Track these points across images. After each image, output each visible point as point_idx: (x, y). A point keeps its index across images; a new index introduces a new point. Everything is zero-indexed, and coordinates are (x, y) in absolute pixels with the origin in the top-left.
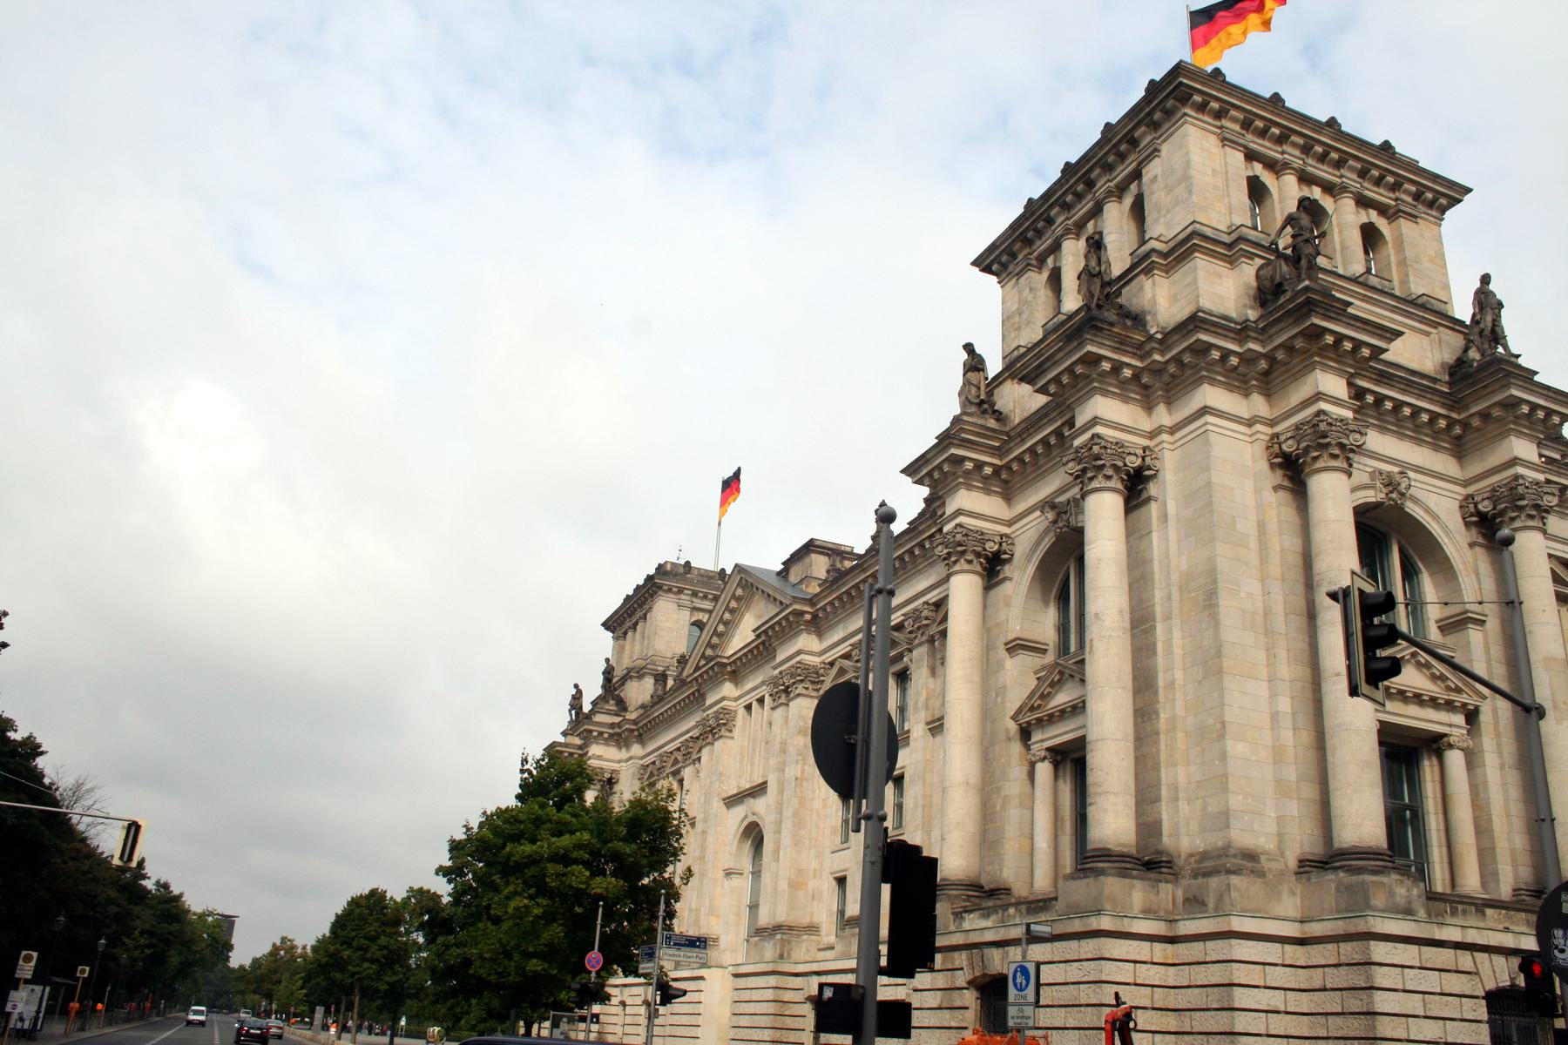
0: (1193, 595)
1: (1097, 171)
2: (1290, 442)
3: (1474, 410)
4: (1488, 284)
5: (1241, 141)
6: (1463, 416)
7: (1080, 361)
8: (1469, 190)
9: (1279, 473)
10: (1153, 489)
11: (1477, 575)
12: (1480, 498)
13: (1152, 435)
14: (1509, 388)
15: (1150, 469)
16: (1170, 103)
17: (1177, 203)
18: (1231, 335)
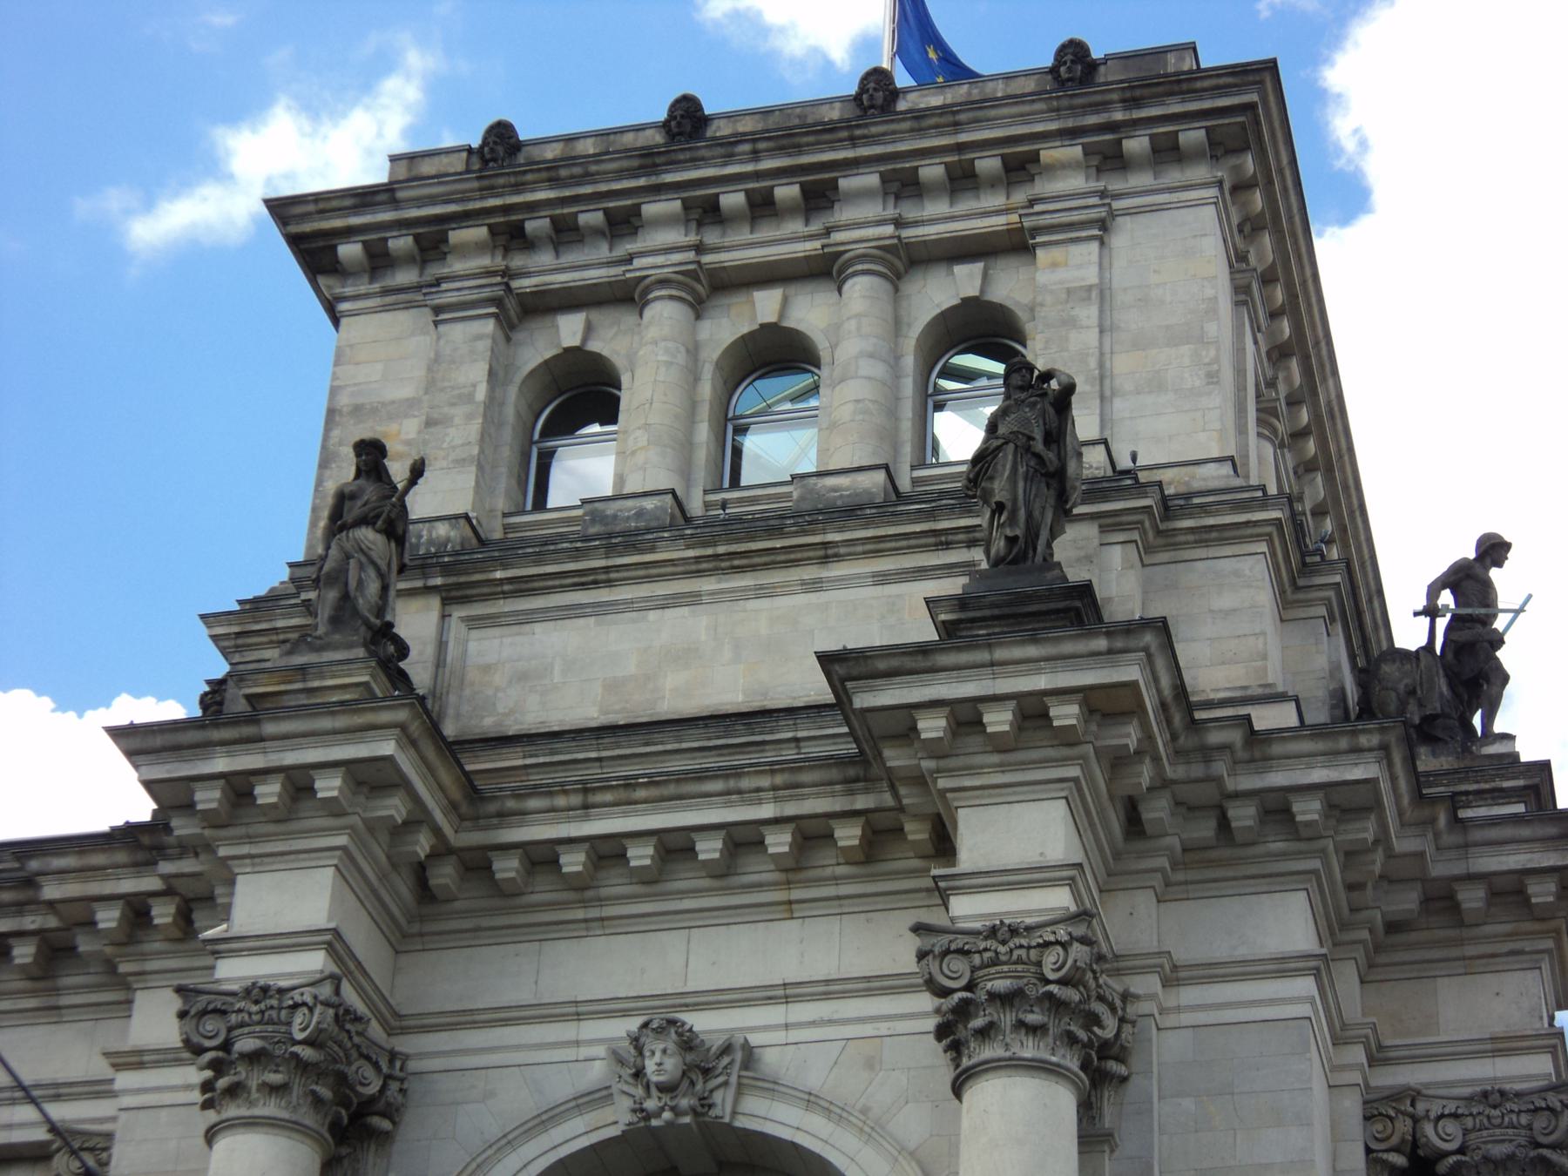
1: (871, 180)
2: (1451, 1127)
7: (1085, 695)
17: (1156, 384)
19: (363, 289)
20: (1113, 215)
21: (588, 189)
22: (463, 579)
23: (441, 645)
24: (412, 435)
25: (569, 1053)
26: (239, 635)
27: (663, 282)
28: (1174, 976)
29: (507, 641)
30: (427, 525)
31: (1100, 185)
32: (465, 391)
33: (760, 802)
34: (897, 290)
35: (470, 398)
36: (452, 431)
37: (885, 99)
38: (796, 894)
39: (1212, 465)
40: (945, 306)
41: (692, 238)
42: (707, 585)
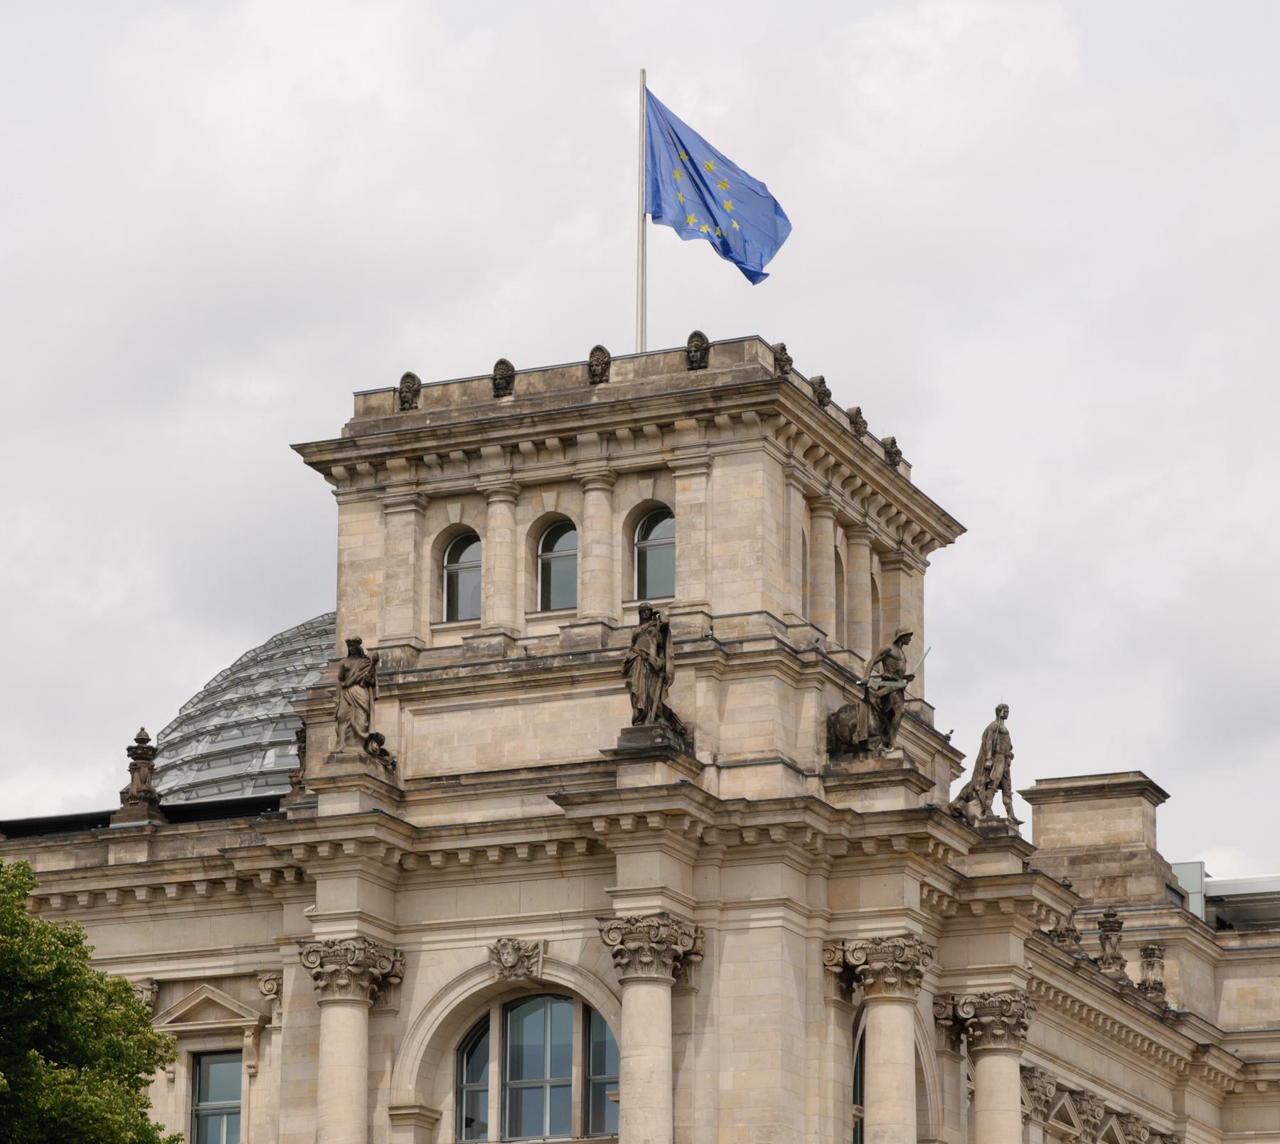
0: (740, 1125)
1: (593, 436)
2: (859, 954)
3: (980, 894)
4: (1005, 717)
5: (805, 479)
6: (965, 897)
8: (964, 530)
9: (833, 982)
10: (695, 978)
11: (942, 1090)
12: (962, 1002)
13: (696, 907)
14: (1031, 884)
15: (696, 954)
16: (749, 415)
18: (828, 815)
19: (348, 489)
20: (712, 457)
21: (452, 441)
22: (408, 692)
23: (400, 724)
24: (381, 581)
25: (473, 943)
26: (308, 711)
27: (496, 492)
28: (724, 908)
29: (432, 722)
30: (390, 650)
31: (706, 441)
32: (404, 557)
33: (541, 832)
34: (612, 492)
35: (405, 562)
36: (399, 582)
37: (603, 369)
38: (564, 868)
39: (756, 616)
40: (636, 503)
41: (508, 467)
42: (521, 696)
